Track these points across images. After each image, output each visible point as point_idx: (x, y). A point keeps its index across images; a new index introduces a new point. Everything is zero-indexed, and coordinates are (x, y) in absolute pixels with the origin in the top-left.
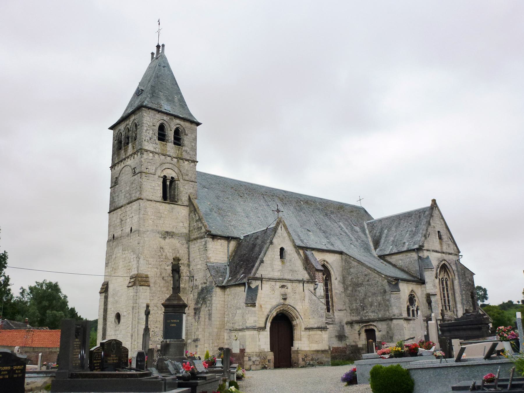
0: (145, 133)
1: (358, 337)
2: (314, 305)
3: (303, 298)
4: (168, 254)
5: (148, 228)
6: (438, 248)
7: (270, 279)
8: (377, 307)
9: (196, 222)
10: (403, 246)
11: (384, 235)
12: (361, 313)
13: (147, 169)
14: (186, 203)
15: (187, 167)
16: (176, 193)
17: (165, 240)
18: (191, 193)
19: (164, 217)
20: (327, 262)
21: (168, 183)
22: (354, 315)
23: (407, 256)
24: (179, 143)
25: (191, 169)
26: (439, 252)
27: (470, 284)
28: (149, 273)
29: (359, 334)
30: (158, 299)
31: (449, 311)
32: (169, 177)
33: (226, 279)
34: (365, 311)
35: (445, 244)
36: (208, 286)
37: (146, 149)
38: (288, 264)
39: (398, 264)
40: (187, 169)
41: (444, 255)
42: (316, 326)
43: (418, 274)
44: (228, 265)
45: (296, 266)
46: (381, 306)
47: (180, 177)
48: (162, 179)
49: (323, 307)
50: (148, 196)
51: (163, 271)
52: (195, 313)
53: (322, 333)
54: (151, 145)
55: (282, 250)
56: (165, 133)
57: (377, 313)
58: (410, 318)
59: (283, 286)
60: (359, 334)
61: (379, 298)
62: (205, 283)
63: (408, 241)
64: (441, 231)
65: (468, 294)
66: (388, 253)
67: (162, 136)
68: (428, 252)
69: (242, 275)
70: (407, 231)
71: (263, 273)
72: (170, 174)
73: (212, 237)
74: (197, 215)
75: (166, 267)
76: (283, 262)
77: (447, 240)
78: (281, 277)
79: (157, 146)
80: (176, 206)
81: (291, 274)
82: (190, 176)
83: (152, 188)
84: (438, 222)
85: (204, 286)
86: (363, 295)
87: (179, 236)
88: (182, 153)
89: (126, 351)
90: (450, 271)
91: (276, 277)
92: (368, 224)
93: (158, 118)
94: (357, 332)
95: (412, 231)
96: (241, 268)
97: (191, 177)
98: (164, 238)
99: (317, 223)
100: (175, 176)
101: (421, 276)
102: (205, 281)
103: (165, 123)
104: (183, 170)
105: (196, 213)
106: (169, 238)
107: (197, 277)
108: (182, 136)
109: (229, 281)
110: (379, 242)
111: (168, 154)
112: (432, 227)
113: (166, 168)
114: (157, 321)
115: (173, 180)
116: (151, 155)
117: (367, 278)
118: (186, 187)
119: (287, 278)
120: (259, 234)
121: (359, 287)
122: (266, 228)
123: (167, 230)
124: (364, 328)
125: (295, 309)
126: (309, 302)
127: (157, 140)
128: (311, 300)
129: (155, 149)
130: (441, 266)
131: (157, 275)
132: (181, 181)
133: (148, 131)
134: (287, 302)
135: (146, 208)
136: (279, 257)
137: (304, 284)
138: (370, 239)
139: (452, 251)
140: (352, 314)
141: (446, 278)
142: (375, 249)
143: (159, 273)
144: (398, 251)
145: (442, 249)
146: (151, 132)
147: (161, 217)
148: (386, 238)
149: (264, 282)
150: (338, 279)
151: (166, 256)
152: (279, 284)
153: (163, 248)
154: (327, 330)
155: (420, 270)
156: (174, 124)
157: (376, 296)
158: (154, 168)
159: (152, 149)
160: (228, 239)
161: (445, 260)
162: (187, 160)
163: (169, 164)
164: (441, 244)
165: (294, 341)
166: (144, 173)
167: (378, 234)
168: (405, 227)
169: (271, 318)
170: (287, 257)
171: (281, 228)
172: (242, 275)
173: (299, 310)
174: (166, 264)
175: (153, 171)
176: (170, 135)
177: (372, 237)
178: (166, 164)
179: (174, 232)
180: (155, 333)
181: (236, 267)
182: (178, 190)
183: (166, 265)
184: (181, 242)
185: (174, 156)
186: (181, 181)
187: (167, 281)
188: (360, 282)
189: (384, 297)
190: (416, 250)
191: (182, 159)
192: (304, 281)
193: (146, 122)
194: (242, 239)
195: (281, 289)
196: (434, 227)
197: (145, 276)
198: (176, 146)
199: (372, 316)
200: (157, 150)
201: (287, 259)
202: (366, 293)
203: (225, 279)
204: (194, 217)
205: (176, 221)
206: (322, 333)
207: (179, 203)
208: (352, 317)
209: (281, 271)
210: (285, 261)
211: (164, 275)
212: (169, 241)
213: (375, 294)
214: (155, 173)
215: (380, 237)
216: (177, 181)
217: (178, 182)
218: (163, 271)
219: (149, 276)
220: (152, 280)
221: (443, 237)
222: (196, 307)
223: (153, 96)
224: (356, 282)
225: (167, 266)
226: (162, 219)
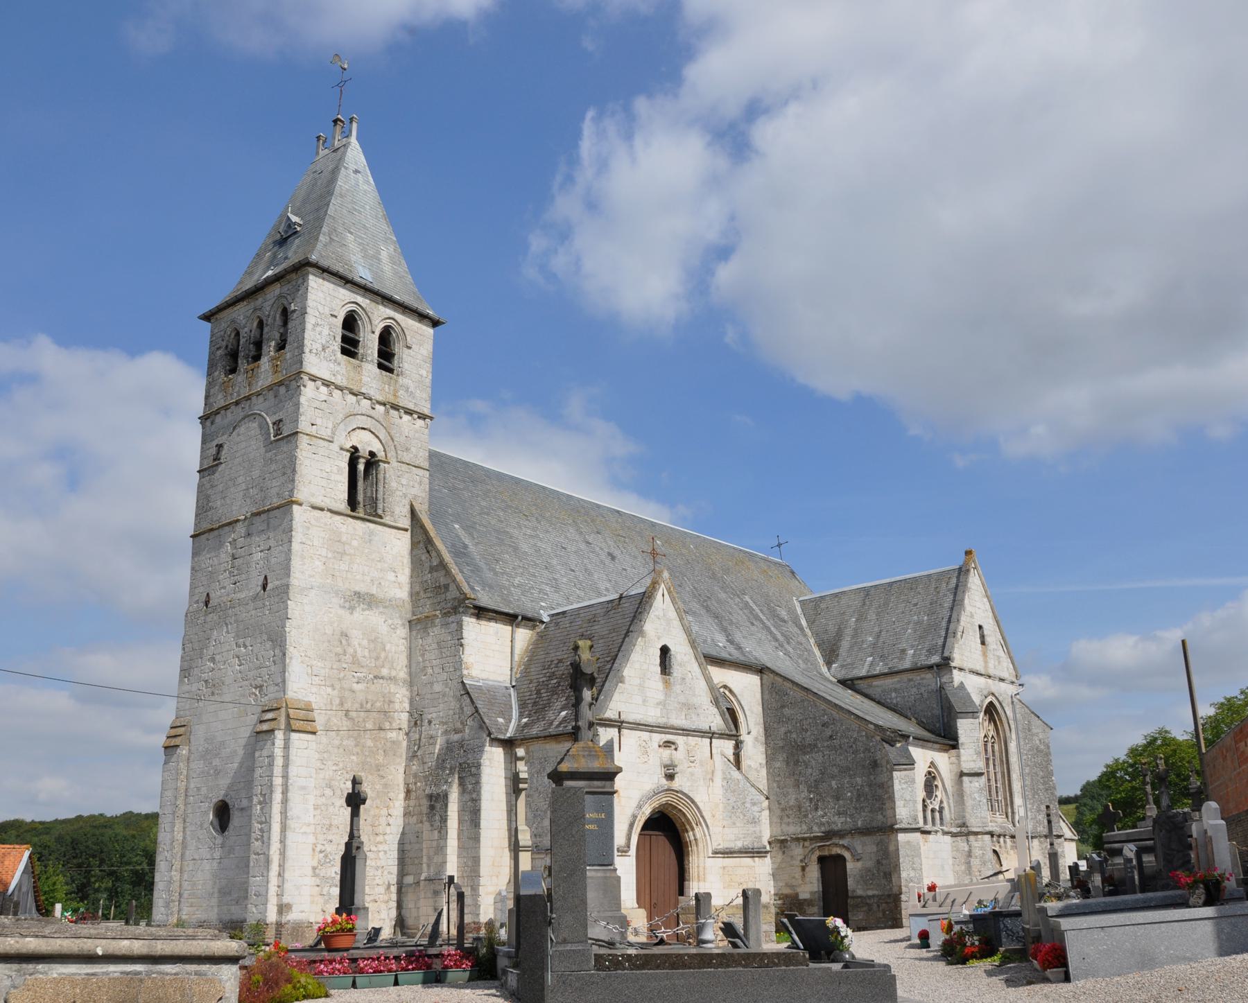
0: (311, 333)
1: (801, 874)
2: (736, 793)
3: (710, 776)
4: (359, 650)
5: (311, 579)
6: (979, 667)
7: (638, 726)
8: (852, 801)
9: (430, 572)
10: (901, 659)
11: (848, 632)
12: (810, 816)
13: (314, 427)
14: (406, 523)
15: (407, 430)
16: (380, 496)
17: (352, 613)
18: (415, 497)
19: (349, 555)
20: (731, 691)
21: (361, 467)
22: (790, 820)
23: (912, 683)
24: (391, 366)
25: (417, 435)
26: (981, 675)
27: (1041, 751)
28: (312, 699)
29: (803, 869)
30: (334, 768)
31: (998, 813)
32: (365, 450)
33: (513, 721)
34: (820, 813)
35: (992, 656)
36: (467, 737)
37: (312, 373)
38: (677, 688)
39: (888, 700)
40: (407, 434)
41: (990, 681)
42: (739, 845)
43: (938, 725)
44: (513, 687)
45: (694, 695)
46: (862, 799)
47: (391, 454)
48: (349, 454)
49: (758, 797)
50: (313, 495)
51: (347, 694)
52: (432, 808)
53: (754, 861)
54: (325, 363)
55: (665, 651)
56: (357, 338)
57: (851, 816)
58: (929, 827)
59: (668, 744)
60: (803, 869)
61: (859, 780)
62: (457, 731)
63: (912, 646)
64: (985, 627)
65: (1036, 773)
66: (863, 673)
67: (350, 346)
68: (962, 673)
69: (564, 713)
70: (909, 623)
71: (622, 707)
72: (367, 443)
73: (477, 611)
74: (434, 554)
75: (355, 684)
76: (667, 684)
77: (995, 647)
78: (662, 721)
79: (339, 369)
80: (380, 528)
81: (684, 714)
82: (414, 453)
83: (325, 475)
84: (978, 604)
85: (456, 737)
86: (816, 773)
87: (385, 607)
88: (396, 391)
89: (946, 940)
90: (1000, 720)
91: (650, 720)
92: (802, 603)
93: (343, 298)
94: (797, 863)
95: (919, 623)
96: (552, 695)
97: (416, 456)
98: (349, 609)
99: (700, 595)
100: (379, 450)
101: (944, 730)
102: (459, 725)
103: (360, 311)
104: (398, 435)
105: (430, 548)
106: (363, 610)
107: (434, 715)
108: (398, 348)
109: (521, 728)
110: (838, 648)
111: (363, 390)
112: (969, 614)
113: (359, 428)
114: (331, 825)
115: (372, 462)
116: (324, 389)
117: (828, 732)
118: (404, 481)
119: (675, 725)
120: (598, 612)
121: (805, 754)
122: (616, 596)
123: (357, 589)
124: (817, 853)
125: (693, 802)
126: (723, 786)
127: (339, 354)
128: (727, 779)
129: (334, 375)
130: (984, 707)
131: (331, 703)
132: (394, 463)
133: (318, 329)
134: (677, 784)
135: (308, 528)
136: (659, 669)
137: (713, 740)
138: (812, 641)
139: (1005, 675)
140: (786, 820)
141: (993, 737)
142: (829, 663)
143: (337, 701)
144: (889, 668)
145: (986, 667)
146: (326, 331)
147: (344, 553)
148: (853, 637)
149: (624, 731)
150: (754, 733)
151: (354, 656)
152: (658, 738)
153: (347, 636)
154: (766, 857)
155: (943, 716)
156: (377, 316)
157: (850, 776)
158: (330, 426)
159: (327, 376)
160: (511, 619)
161: (993, 694)
162: (409, 412)
163: (365, 417)
164: (985, 654)
165: (686, 883)
166: (307, 435)
167: (832, 629)
168: (903, 613)
169: (641, 824)
170: (677, 670)
171: (663, 595)
172: (564, 713)
173: (700, 805)
174: (354, 676)
175: (326, 433)
176: (370, 343)
177: (816, 635)
178: (358, 416)
179: (373, 595)
180: (326, 856)
181: (538, 692)
182: (384, 487)
183: (356, 680)
184: (390, 622)
185: (380, 399)
186: (394, 463)
187: (356, 720)
188: (808, 741)
189: (872, 777)
190: (935, 668)
191: (395, 407)
192: (713, 733)
193: (315, 304)
194: (545, 620)
195: (661, 750)
196: (972, 616)
197: (303, 707)
198: (384, 372)
199: (839, 825)
200: (339, 380)
201: (675, 674)
202: (825, 768)
203: (510, 722)
204: (423, 558)
205: (379, 565)
206: (754, 861)
207: (387, 520)
208: (783, 825)
209: (663, 704)
210: (672, 680)
211: (347, 706)
212: (361, 617)
213: (849, 769)
214: (333, 438)
215: (839, 635)
216: (385, 462)
217: (386, 465)
218: (347, 694)
219: (314, 706)
220: (320, 720)
221: (988, 639)
222: (434, 790)
223: (330, 242)
224: (799, 740)
225: (358, 683)
226: (346, 558)
